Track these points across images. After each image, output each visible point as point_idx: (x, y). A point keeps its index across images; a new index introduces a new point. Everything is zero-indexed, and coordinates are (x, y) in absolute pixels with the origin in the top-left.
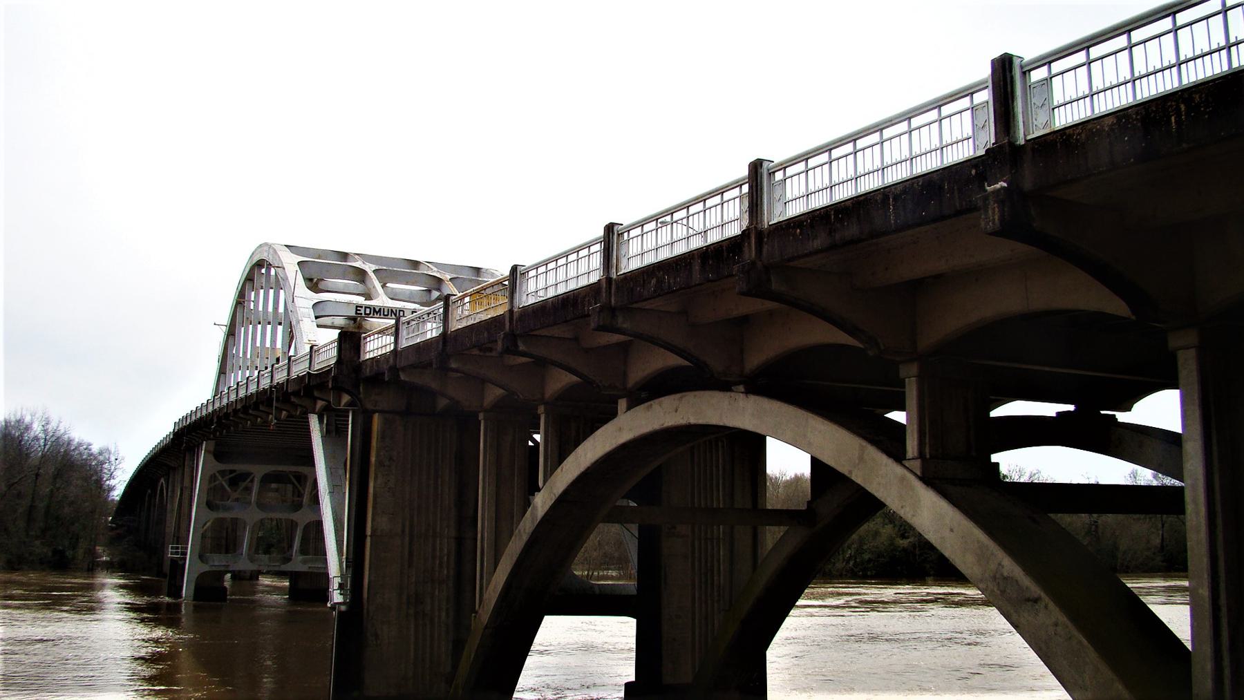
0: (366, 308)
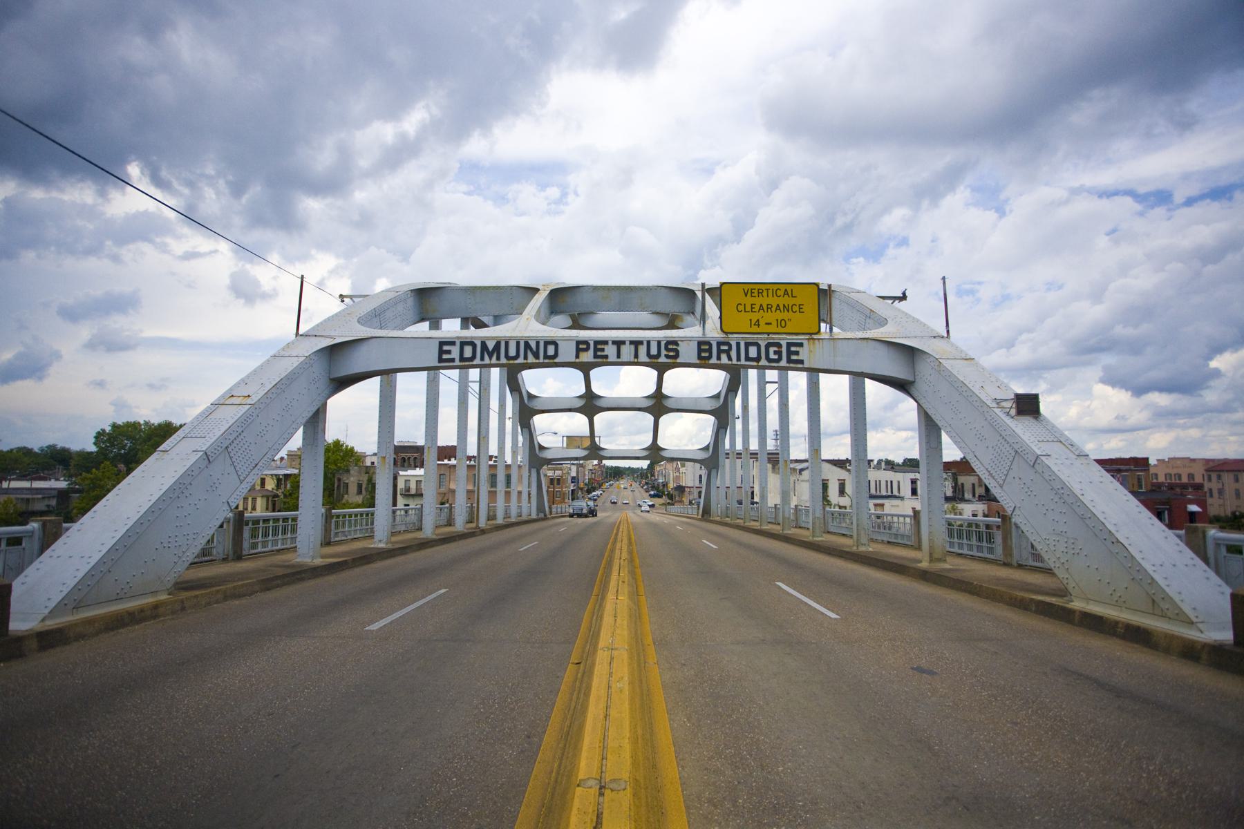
0: (463, 344)
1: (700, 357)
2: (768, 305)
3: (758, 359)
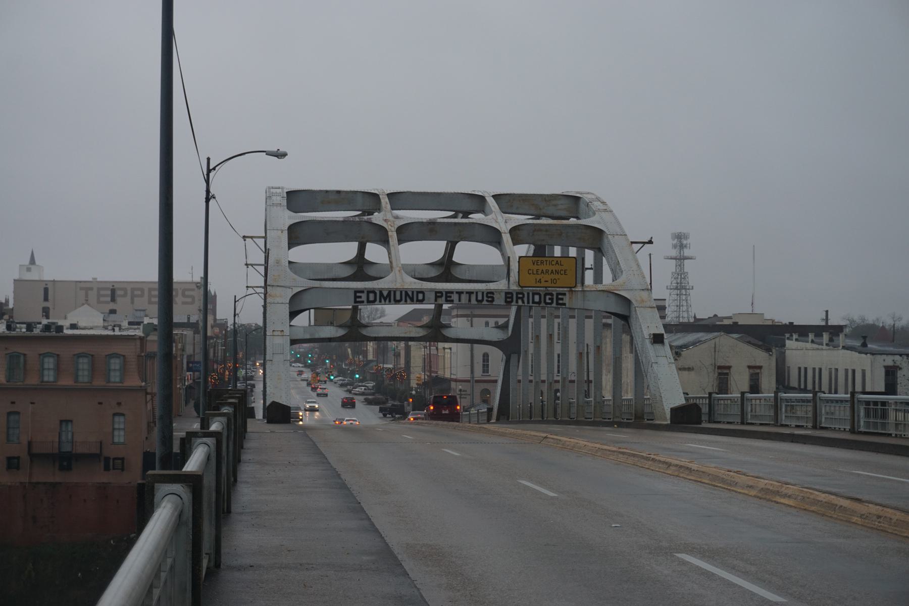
1: (506, 301)
2: (546, 270)
3: (539, 303)
